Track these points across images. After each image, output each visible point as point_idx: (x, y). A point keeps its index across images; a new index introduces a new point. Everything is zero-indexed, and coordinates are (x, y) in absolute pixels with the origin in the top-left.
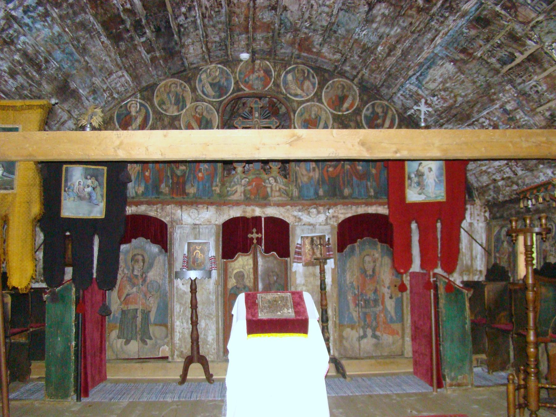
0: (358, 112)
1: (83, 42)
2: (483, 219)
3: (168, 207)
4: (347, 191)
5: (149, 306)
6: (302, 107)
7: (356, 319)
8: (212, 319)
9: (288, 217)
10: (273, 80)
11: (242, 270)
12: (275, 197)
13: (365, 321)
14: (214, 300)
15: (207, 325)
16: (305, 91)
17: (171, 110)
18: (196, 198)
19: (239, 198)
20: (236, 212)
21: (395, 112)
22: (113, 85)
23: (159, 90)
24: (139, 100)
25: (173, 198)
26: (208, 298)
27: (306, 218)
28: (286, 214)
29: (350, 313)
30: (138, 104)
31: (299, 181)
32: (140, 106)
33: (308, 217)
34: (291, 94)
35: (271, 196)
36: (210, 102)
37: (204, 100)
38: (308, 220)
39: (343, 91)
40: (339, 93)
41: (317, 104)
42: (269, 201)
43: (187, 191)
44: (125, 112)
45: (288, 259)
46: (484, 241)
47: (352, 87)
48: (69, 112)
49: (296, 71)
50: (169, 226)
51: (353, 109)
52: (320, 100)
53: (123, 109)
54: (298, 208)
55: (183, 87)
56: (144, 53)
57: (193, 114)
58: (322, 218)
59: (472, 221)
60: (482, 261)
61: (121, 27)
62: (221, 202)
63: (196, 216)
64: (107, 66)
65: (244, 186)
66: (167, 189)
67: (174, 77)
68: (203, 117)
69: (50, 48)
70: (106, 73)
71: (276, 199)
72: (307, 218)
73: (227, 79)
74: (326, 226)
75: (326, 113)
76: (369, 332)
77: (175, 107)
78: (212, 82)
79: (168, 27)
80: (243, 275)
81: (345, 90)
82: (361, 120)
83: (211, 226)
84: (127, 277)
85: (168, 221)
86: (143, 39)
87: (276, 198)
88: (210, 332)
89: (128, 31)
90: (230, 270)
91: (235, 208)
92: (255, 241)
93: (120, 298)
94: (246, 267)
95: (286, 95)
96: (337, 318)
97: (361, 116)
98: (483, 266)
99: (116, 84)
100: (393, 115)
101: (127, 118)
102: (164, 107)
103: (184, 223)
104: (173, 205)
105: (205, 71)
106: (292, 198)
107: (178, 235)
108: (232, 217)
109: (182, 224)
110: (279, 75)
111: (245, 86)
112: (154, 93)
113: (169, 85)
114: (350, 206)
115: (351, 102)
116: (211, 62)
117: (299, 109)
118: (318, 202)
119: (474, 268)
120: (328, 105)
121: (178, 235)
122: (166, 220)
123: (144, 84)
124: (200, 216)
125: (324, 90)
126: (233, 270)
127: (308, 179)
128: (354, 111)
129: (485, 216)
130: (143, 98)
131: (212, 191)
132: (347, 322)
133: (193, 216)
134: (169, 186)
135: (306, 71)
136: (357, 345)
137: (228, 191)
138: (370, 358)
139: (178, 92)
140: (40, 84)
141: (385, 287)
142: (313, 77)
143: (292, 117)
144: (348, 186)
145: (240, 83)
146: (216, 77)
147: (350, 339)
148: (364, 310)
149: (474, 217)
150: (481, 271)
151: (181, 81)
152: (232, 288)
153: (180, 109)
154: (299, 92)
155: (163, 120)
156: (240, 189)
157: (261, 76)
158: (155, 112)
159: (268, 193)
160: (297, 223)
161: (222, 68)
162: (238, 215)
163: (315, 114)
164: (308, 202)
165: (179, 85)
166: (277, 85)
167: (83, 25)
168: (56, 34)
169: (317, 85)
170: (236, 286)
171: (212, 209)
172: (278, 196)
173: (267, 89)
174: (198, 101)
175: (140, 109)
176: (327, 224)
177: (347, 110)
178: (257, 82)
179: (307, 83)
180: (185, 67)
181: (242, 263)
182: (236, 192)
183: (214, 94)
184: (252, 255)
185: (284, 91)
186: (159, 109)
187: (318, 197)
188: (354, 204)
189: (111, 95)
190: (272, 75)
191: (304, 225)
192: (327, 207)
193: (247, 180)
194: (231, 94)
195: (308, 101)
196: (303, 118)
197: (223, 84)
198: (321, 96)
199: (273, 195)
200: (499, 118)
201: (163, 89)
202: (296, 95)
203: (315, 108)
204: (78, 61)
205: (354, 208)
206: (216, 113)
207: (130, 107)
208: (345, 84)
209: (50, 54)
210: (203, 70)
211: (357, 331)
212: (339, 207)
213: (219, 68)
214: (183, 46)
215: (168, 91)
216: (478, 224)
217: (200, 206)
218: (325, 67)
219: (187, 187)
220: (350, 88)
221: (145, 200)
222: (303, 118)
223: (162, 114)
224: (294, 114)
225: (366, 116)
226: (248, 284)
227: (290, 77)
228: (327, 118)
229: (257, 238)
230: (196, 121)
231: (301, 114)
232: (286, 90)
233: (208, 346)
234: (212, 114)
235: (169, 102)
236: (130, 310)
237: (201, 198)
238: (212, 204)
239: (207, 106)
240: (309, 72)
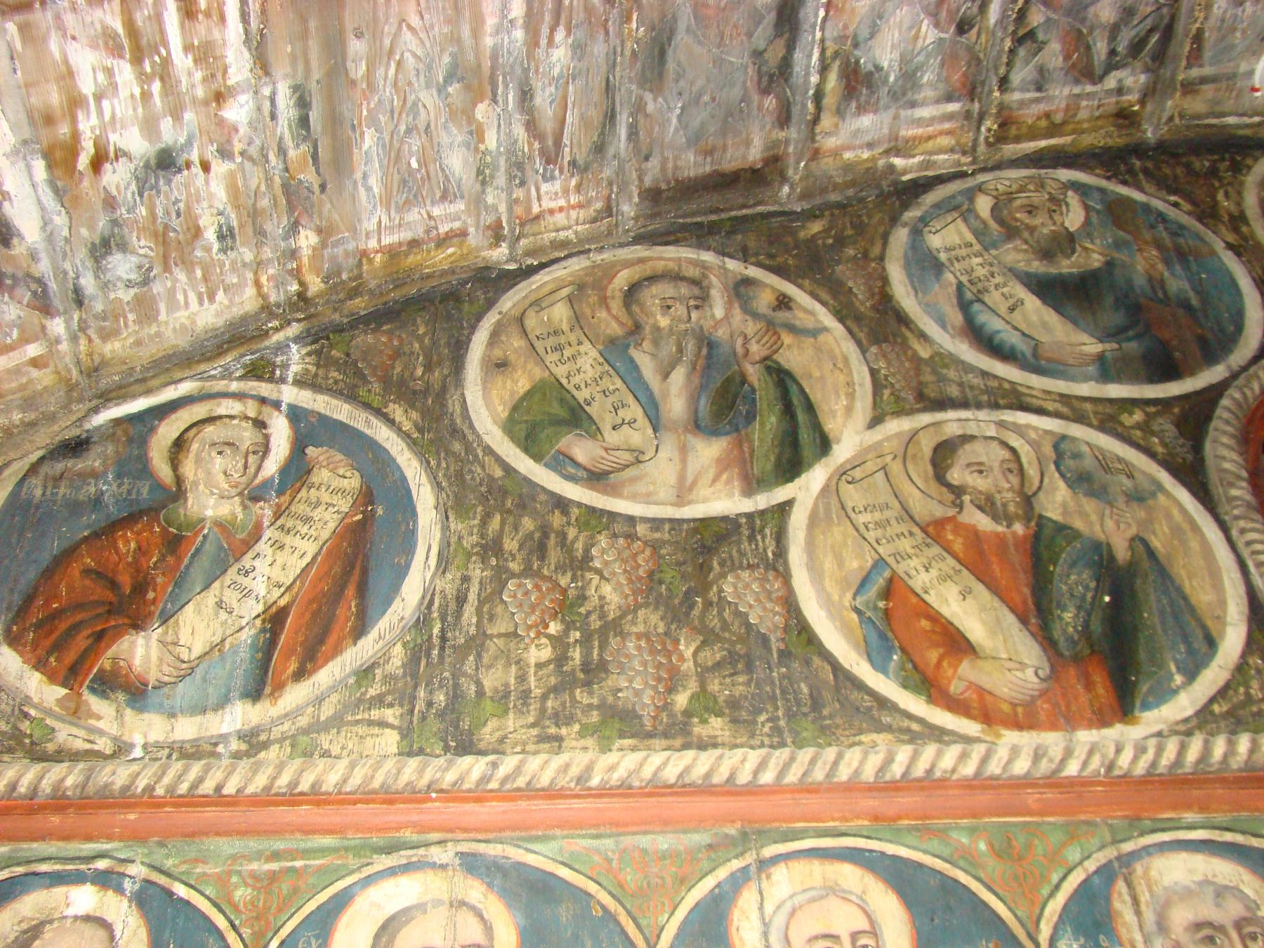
17: (662, 469)
24: (290, 394)
30: (281, 432)
36: (1073, 409)
44: (109, 488)
53: (92, 461)
57: (928, 506)
77: (708, 451)
78: (1037, 267)
102: (582, 450)
123: (376, 223)
139: (721, 333)
151: (731, 264)
153: (764, 464)
155: (581, 565)
158: (481, 493)
161: (1102, 191)
174: (941, 404)
175: (297, 471)
183: (1093, 347)
186: (524, 464)
201: (560, 313)
206: (1183, 495)
207: (180, 445)
210: (931, 198)
213: (1075, 186)
223: (562, 504)
230: (978, 561)
235: (634, 411)
239: (1060, 441)
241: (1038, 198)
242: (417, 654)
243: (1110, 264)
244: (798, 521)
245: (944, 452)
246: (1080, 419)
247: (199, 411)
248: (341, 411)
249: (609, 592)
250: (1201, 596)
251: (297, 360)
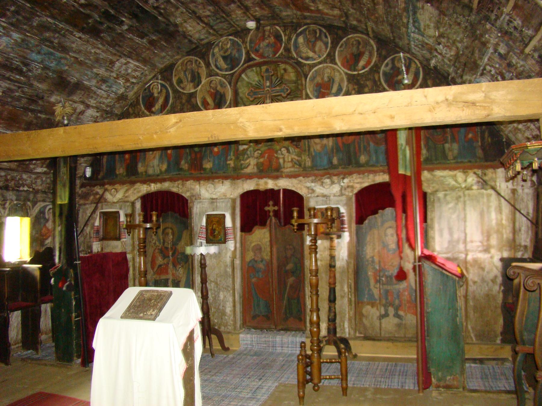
0: (376, 69)
1: (56, 41)
2: (529, 183)
3: (188, 183)
4: (363, 159)
5: (179, 276)
6: (313, 70)
7: (377, 297)
8: (229, 291)
9: (301, 189)
10: (283, 45)
11: (259, 243)
12: (287, 168)
13: (387, 299)
14: (231, 273)
15: (225, 297)
16: (317, 53)
17: (188, 87)
18: (212, 173)
19: (252, 171)
20: (249, 186)
21: (419, 65)
22: (123, 72)
23: (177, 69)
24: (160, 81)
25: (192, 174)
26: (226, 272)
27: (319, 189)
28: (299, 186)
29: (370, 290)
31: (312, 149)
32: (161, 87)
33: (322, 188)
34: (302, 58)
35: (284, 167)
37: (217, 75)
38: (322, 191)
39: (358, 48)
40: (355, 49)
41: (330, 65)
42: (282, 172)
43: (204, 166)
44: (148, 94)
46: (531, 211)
47: (369, 42)
48: (83, 102)
49: (307, 33)
50: (189, 201)
51: (369, 67)
52: (333, 61)
53: (147, 91)
54: (310, 178)
55: (198, 63)
56: (137, 40)
57: (208, 89)
58: (336, 189)
59: (515, 187)
60: (528, 234)
61: (90, 21)
62: (236, 175)
63: (213, 190)
64: (102, 57)
65: (257, 158)
66: (186, 165)
67: (189, 55)
68: (217, 91)
69: (21, 53)
70: (106, 63)
71: (288, 170)
72: (320, 189)
73: (239, 50)
74: (341, 198)
75: (341, 74)
76: (391, 311)
77: (192, 84)
78: (224, 55)
79: (144, 11)
81: (360, 47)
82: (379, 77)
83: (227, 200)
84: (159, 249)
85: (189, 196)
86: (125, 27)
87: (288, 168)
88: (228, 303)
89: (102, 23)
91: (248, 181)
92: (271, 214)
93: (153, 268)
95: (297, 59)
96: (353, 295)
97: (379, 73)
98: (528, 240)
99: (126, 70)
100: (417, 69)
101: (151, 99)
102: (182, 85)
103: (202, 198)
104: (192, 181)
105: (218, 45)
106: (305, 169)
107: (198, 210)
108: (245, 191)
109: (200, 199)
110: (290, 39)
111: (256, 56)
112: (172, 73)
113: (185, 63)
114: (366, 174)
115: (367, 58)
116: (222, 36)
117: (311, 73)
118: (331, 171)
119: (517, 243)
120: (343, 65)
121: (198, 210)
122: (186, 195)
124: (216, 190)
125: (338, 49)
126: (251, 243)
127: (321, 147)
128: (371, 69)
129: (532, 181)
130: (163, 79)
131: (227, 165)
132: (367, 299)
133: (210, 192)
134: (188, 163)
135: (318, 31)
136: (378, 324)
137: (242, 165)
138: (388, 340)
140: (31, 85)
141: (409, 262)
142: (326, 37)
143: (304, 82)
144: (365, 152)
145: (251, 52)
146: (227, 50)
147: (370, 317)
148: (385, 287)
149: (517, 182)
150: (526, 247)
152: (250, 261)
154: (311, 54)
155: (182, 98)
156: (253, 162)
157: (271, 43)
158: (175, 91)
159: (280, 164)
160: (310, 195)
162: (252, 188)
163: (328, 77)
164: (321, 172)
165: (194, 62)
166: (288, 50)
167: (44, 27)
168: (19, 40)
169: (329, 45)
170: (254, 259)
171: (227, 183)
172: (290, 167)
173: (277, 55)
175: (161, 90)
176: (342, 195)
177: (364, 68)
178: (267, 49)
179: (319, 44)
180: (195, 44)
181: (261, 236)
182: (249, 164)
183: (226, 67)
184: (268, 228)
185: (295, 56)
187: (332, 166)
188: (370, 172)
189: (127, 80)
190: (282, 40)
191: (318, 196)
192: (342, 176)
193: (260, 152)
194: (243, 64)
195: (320, 63)
196: (316, 81)
197: (235, 55)
198: (334, 56)
199: (286, 166)
200: (500, 65)
201: (180, 67)
202: (307, 58)
203: (327, 70)
204: (61, 58)
205: (371, 176)
206: (229, 86)
208: (360, 40)
209: (26, 58)
210: (215, 44)
211: (377, 309)
212: (355, 176)
213: (230, 40)
214: (176, 25)
215: (184, 69)
216: (523, 190)
217: (216, 180)
218: (336, 24)
219: (204, 162)
220: (367, 43)
221: (167, 177)
222: (316, 81)
223: (180, 92)
224: (306, 78)
225: (385, 74)
227: (301, 40)
228: (342, 80)
229: (274, 211)
231: (313, 78)
232: (297, 54)
233: (226, 317)
234: (225, 87)
235: (186, 80)
236: (162, 279)
237: (216, 173)
238: (226, 178)
239: (220, 80)
240: (321, 31)
241: (226, 42)
242: (171, 108)
243: (231, 53)
244: (198, 92)
245: (211, 82)
246: (222, 77)
247: (153, 85)
248: (164, 83)
249: (184, 101)
250: (227, 98)
251: (160, 77)
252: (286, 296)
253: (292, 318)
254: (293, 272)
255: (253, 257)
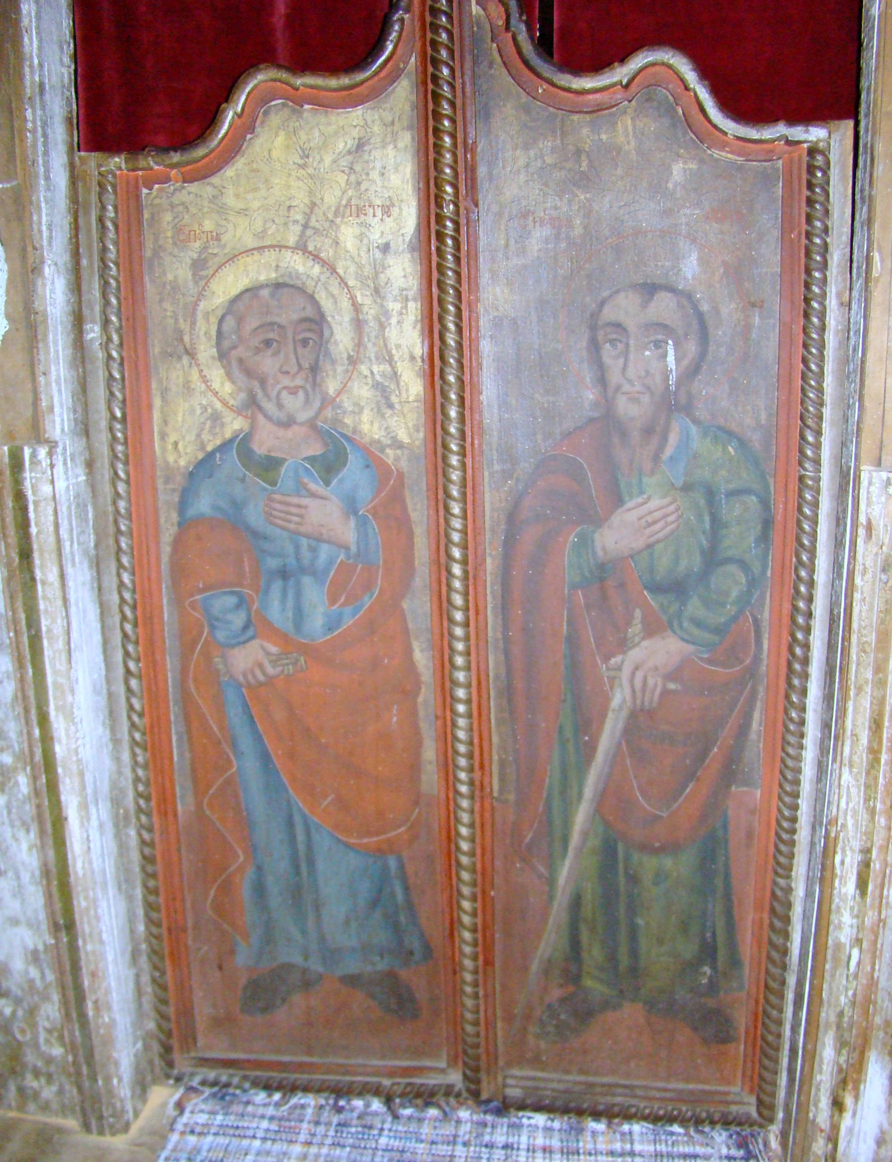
45: (828, 137)
80: (316, 323)
90: (178, 269)
94: (348, 234)
152: (206, 465)
170: (242, 445)
184: (403, 94)
226: (370, 427)
252: (581, 816)
253: (631, 1013)
254: (676, 588)
255: (235, 424)
